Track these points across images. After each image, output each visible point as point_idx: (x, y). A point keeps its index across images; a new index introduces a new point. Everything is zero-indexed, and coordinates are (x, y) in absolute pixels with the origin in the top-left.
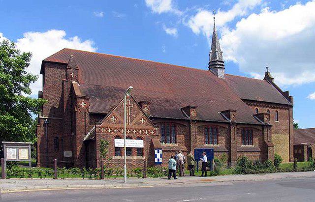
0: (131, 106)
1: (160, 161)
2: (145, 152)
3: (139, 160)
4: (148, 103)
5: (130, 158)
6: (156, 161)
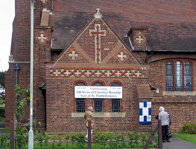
0: (102, 33)
1: (149, 120)
2: (124, 105)
3: (114, 119)
4: (142, 30)
5: (98, 115)
6: (141, 119)
